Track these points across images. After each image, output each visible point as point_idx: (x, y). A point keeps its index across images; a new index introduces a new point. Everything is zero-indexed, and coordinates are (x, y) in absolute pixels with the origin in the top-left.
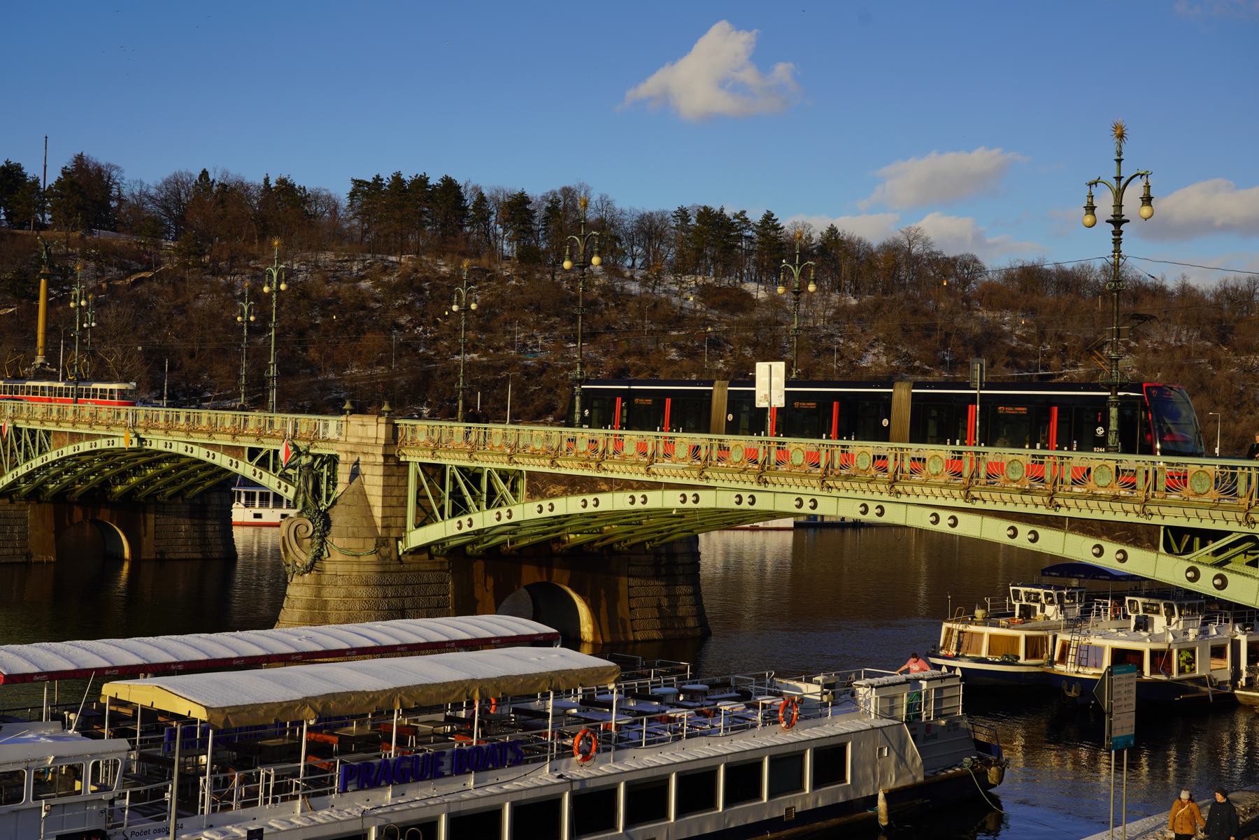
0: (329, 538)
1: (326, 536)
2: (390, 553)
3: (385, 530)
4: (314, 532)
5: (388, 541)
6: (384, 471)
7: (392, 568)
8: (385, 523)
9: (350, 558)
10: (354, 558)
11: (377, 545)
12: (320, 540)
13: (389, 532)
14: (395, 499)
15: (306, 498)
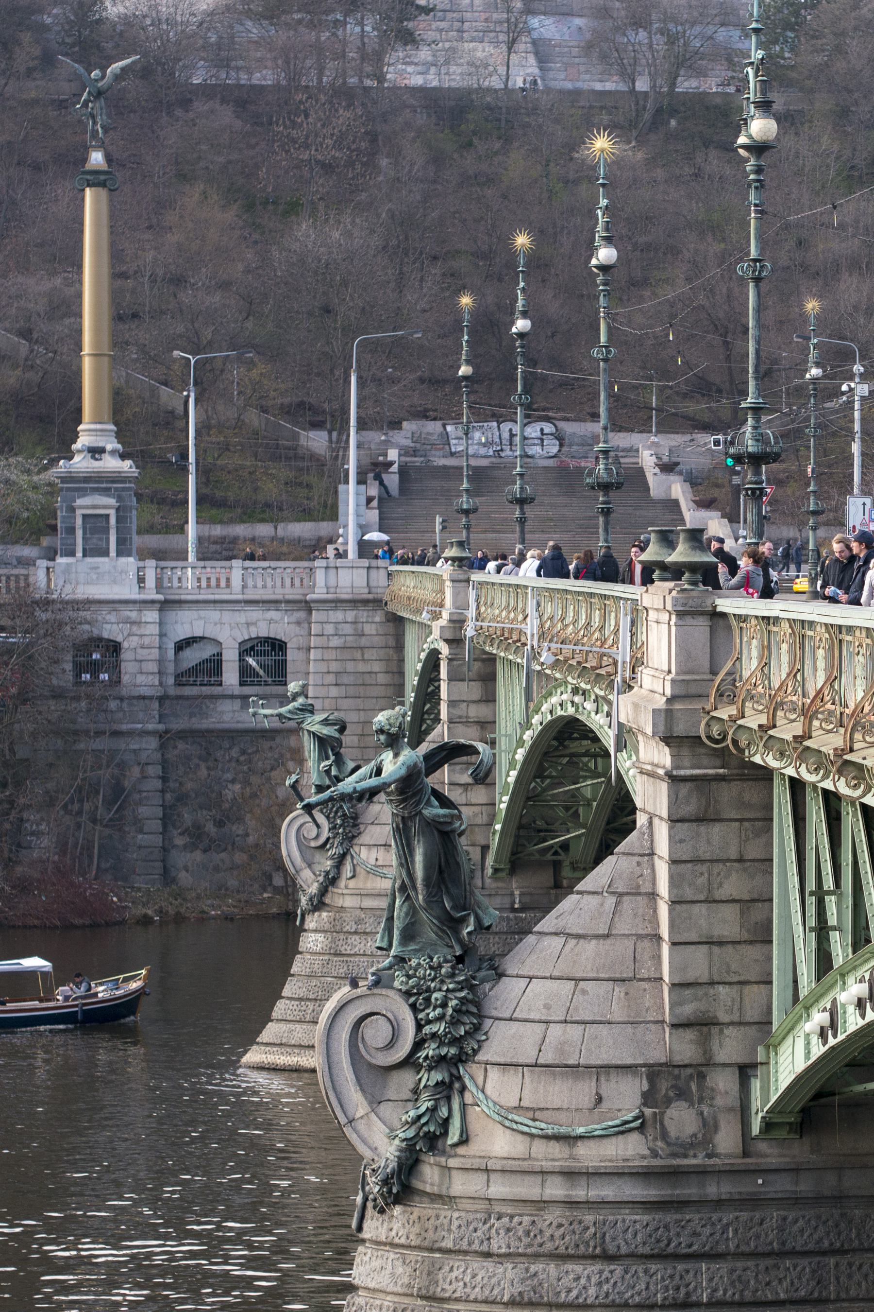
0: (471, 1073)
1: (462, 1058)
2: (710, 1126)
3: (689, 1035)
4: (418, 1045)
5: (702, 1076)
6: (674, 801)
7: (712, 1190)
8: (688, 1010)
9: (540, 1148)
10: (556, 1149)
11: (648, 1098)
12: (437, 1076)
13: (704, 1042)
14: (730, 912)
15: (412, 911)
